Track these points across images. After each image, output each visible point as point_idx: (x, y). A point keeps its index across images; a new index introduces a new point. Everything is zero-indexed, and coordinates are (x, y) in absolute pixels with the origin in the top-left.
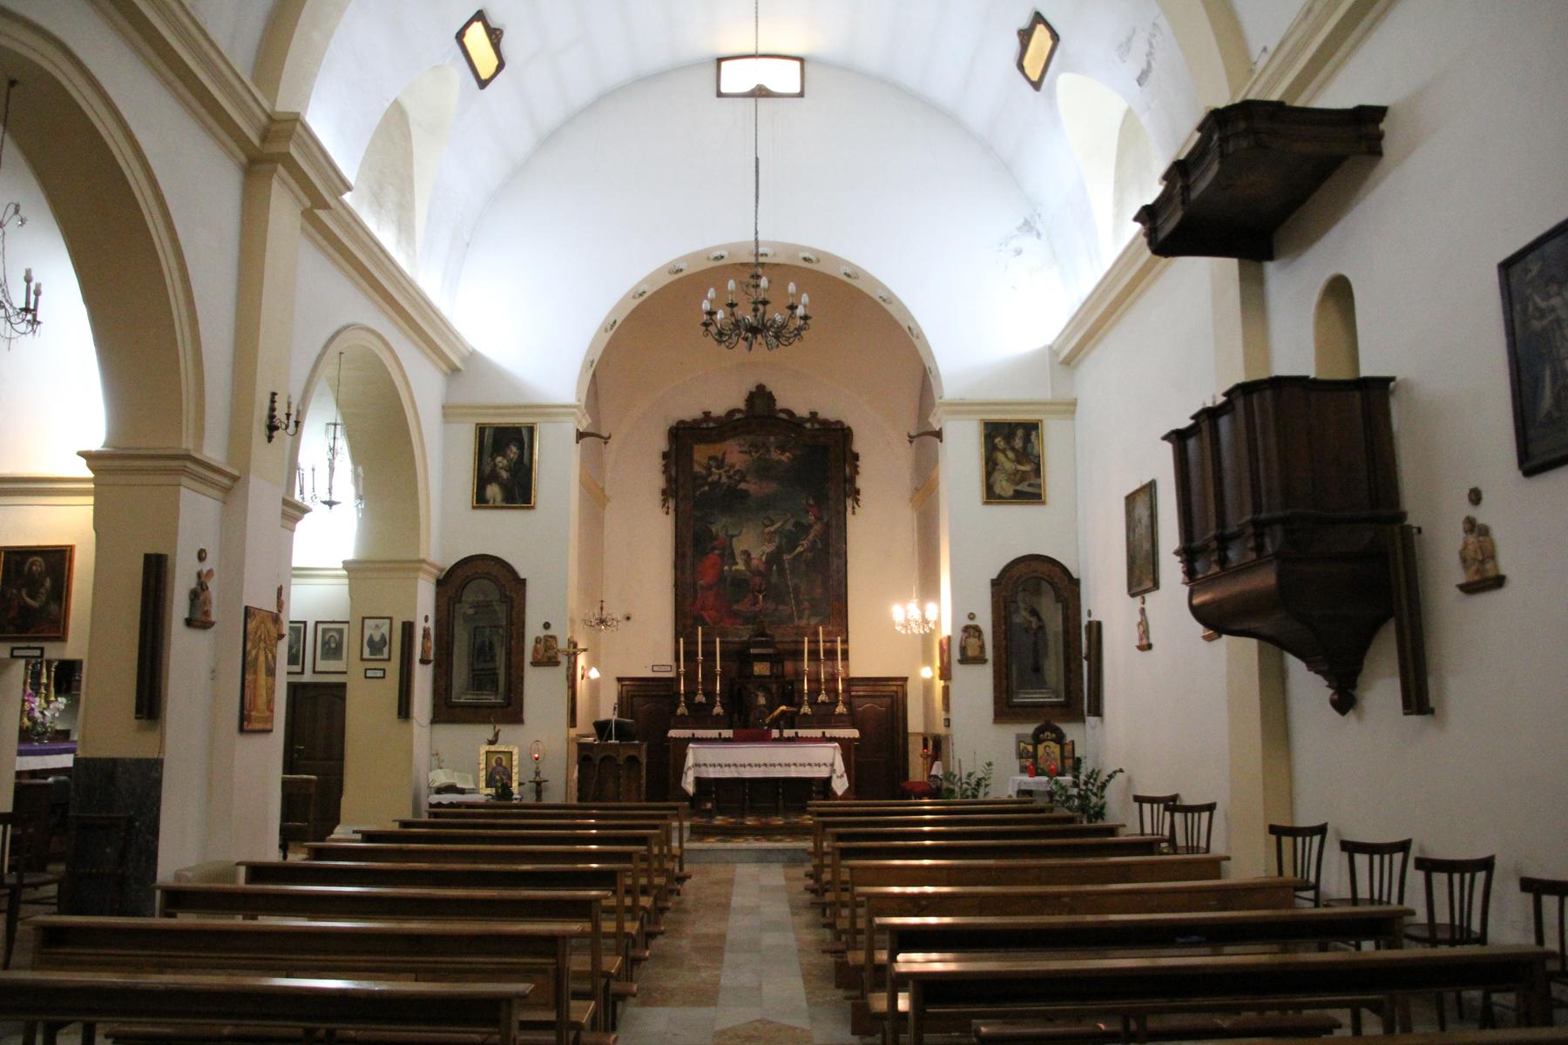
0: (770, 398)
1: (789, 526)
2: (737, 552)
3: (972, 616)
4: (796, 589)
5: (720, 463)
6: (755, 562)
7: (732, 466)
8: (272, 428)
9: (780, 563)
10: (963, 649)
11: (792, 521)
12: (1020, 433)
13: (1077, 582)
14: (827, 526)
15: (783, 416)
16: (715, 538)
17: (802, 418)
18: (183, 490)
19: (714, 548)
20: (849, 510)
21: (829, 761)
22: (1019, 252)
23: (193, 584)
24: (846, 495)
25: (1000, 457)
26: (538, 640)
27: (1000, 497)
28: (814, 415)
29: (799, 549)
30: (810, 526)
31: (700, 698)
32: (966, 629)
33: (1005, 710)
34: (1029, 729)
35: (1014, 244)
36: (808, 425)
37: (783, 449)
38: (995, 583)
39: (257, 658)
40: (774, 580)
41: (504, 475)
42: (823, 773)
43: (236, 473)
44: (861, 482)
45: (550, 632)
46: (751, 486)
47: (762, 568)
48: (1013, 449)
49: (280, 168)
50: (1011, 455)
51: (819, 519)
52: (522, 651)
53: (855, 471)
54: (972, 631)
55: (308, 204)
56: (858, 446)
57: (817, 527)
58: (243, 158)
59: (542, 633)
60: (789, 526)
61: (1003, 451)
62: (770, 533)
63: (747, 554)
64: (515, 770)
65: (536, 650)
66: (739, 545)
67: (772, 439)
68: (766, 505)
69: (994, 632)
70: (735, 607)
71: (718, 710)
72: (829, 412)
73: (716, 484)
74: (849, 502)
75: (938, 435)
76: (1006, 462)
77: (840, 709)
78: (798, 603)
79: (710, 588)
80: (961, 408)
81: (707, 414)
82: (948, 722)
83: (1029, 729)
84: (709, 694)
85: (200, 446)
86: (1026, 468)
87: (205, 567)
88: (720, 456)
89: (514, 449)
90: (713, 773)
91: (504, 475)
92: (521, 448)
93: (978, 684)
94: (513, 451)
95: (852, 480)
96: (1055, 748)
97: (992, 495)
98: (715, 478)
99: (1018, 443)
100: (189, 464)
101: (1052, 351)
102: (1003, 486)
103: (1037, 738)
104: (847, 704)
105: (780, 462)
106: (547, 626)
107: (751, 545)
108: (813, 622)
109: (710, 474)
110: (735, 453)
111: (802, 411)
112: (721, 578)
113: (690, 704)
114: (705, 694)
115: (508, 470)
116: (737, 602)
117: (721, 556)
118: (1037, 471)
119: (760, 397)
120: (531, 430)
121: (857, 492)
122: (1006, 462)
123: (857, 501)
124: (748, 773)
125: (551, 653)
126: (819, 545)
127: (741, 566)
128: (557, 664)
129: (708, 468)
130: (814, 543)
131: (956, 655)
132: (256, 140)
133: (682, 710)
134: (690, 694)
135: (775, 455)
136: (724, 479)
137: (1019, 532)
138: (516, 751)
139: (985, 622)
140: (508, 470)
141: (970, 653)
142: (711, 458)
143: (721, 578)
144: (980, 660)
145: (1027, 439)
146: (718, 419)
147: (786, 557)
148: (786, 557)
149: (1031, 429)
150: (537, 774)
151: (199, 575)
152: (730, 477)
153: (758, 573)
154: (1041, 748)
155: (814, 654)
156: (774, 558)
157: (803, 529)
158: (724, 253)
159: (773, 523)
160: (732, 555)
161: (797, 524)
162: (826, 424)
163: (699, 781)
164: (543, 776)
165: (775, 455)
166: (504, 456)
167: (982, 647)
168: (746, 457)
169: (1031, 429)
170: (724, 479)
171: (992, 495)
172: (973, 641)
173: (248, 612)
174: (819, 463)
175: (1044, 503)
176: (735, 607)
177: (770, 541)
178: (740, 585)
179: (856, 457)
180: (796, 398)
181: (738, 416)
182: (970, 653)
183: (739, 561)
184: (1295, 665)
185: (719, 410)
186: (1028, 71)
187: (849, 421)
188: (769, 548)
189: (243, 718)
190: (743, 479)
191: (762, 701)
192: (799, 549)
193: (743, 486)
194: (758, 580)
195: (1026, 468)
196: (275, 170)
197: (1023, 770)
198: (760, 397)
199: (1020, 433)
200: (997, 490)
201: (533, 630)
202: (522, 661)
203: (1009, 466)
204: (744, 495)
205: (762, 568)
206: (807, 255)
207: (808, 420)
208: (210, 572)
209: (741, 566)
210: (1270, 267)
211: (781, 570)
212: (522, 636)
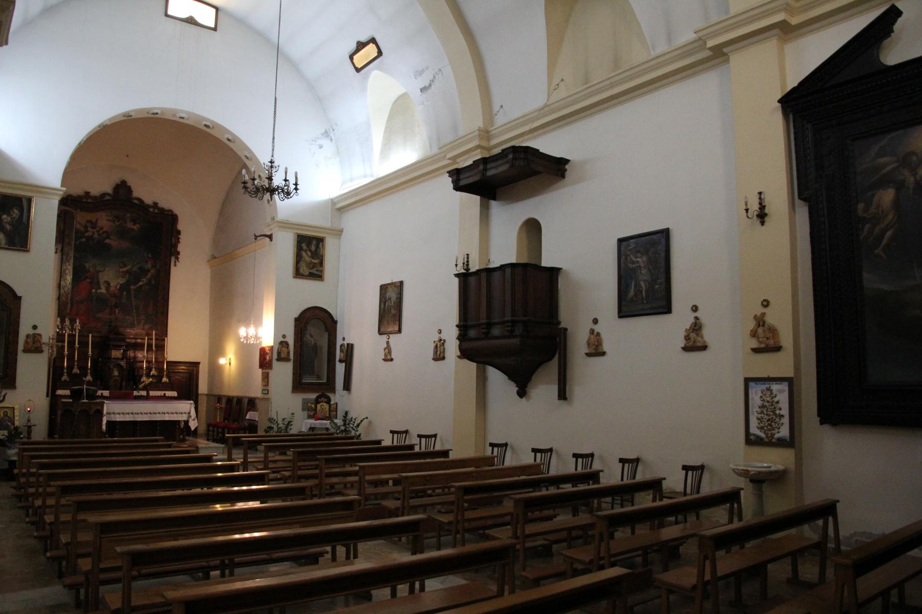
0: (129, 190)
1: (135, 269)
2: (102, 281)
3: (284, 336)
5: (94, 225)
6: (112, 289)
7: (102, 228)
10: (279, 353)
12: (314, 242)
13: (336, 322)
15: (136, 202)
17: (148, 205)
19: (86, 278)
20: (172, 263)
21: (187, 411)
22: (321, 147)
24: (171, 255)
25: (304, 254)
26: (28, 336)
27: (302, 275)
28: (155, 204)
29: (141, 283)
30: (149, 271)
31: (76, 370)
32: (281, 343)
33: (298, 386)
34: (313, 396)
35: (319, 142)
36: (151, 210)
37: (134, 222)
38: (296, 320)
41: (8, 227)
42: (184, 417)
44: (180, 248)
45: (37, 331)
46: (113, 242)
48: (310, 251)
50: (309, 253)
52: (17, 343)
53: (178, 241)
54: (283, 344)
56: (180, 227)
59: (31, 332)
61: (306, 251)
63: (108, 283)
64: (16, 418)
65: (26, 342)
67: (129, 215)
69: (295, 346)
70: (98, 315)
71: (89, 378)
72: (164, 204)
73: (87, 238)
74: (173, 259)
75: (270, 237)
76: (306, 256)
77: (165, 379)
80: (286, 225)
81: (87, 193)
82: (266, 391)
83: (313, 396)
84: (83, 369)
86: (316, 261)
88: (94, 220)
89: (16, 211)
90: (118, 418)
91: (8, 227)
92: (22, 211)
93: (283, 373)
94: (16, 212)
95: (176, 246)
96: (326, 406)
97: (298, 274)
98: (90, 234)
99: (313, 248)
101: (333, 202)
102: (304, 270)
103: (317, 401)
104: (168, 376)
105: (132, 229)
106: (35, 327)
107: (111, 278)
108: (147, 327)
109: (87, 231)
110: (104, 220)
111: (148, 200)
113: (69, 373)
114: (79, 368)
115: (11, 224)
118: (321, 263)
119: (123, 188)
120: (29, 200)
121: (178, 253)
122: (306, 256)
123: (177, 258)
124: (139, 418)
125: (38, 345)
126: (153, 282)
127: (103, 290)
128: (41, 351)
129: (86, 227)
130: (150, 281)
131: (275, 356)
133: (65, 377)
134: (70, 367)
135: (130, 225)
136: (96, 236)
137: (310, 294)
138: (16, 407)
139: (291, 340)
140: (11, 224)
141: (283, 356)
142: (88, 222)
144: (287, 359)
145: (317, 247)
146: (95, 198)
147: (132, 287)
148: (132, 287)
149: (320, 241)
150: (29, 421)
152: (99, 235)
154: (319, 406)
155: (150, 346)
156: (124, 288)
157: (144, 272)
158: (159, 112)
159: (125, 266)
160: (98, 283)
161: (141, 268)
162: (162, 210)
163: (109, 423)
164: (32, 422)
165: (130, 225)
166: (9, 215)
167: (288, 353)
168: (111, 224)
169: (320, 241)
170: (96, 236)
171: (298, 274)
172: (284, 349)
174: (156, 235)
175: (323, 280)
176: (98, 315)
177: (123, 277)
179: (179, 233)
180: (145, 192)
181: (108, 198)
182: (283, 356)
183: (102, 286)
184: (495, 375)
185: (95, 191)
186: (355, 61)
187: (177, 211)
188: (122, 281)
190: (108, 237)
191: (116, 373)
192: (141, 283)
193: (107, 241)
195: (316, 261)
197: (309, 417)
198: (123, 188)
199: (314, 242)
200: (301, 271)
201: (25, 330)
202: (17, 349)
203: (308, 259)
206: (208, 124)
207: (151, 207)
209: (103, 290)
210: (493, 203)
212: (16, 333)
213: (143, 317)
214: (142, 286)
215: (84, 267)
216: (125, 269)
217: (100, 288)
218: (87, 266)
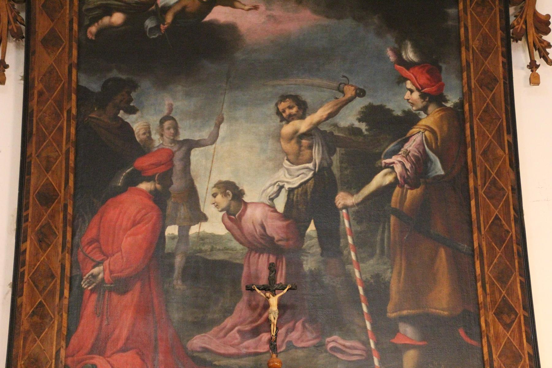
1: (350, 118)
2: (204, 188)
4: (378, 291)
6: (254, 215)
9: (328, 217)
11: (360, 104)
14: (457, 116)
16: (143, 149)
29: (381, 179)
30: (410, 120)
40: (309, 264)
47: (275, 228)
51: (435, 98)
57: (430, 119)
60: (350, 118)
62: (299, 137)
63: (233, 192)
66: (209, 169)
68: (290, 60)
70: (197, 342)
74: (520, 56)
78: (385, 328)
79: (121, 286)
112: (157, 253)
116: (201, 326)
117: (159, 198)
123: (542, 49)
126: (438, 169)
127: (214, 225)
130: (421, 163)
143: (157, 253)
147: (343, 199)
148: (343, 199)
153: (263, 244)
156: (311, 204)
157: (391, 126)
159: (304, 110)
160: (191, 194)
161: (375, 115)
176: (197, 342)
178: (212, 276)
183: (208, 208)
188: (296, 176)
192: (381, 179)
194: (262, 263)
204: (223, 41)
205: (275, 228)
209: (214, 225)
211: (330, 238)
213: (408, 332)
214: (385, 192)
215: (127, 129)
216: (303, 126)
217: (204, 218)
218: (137, 124)
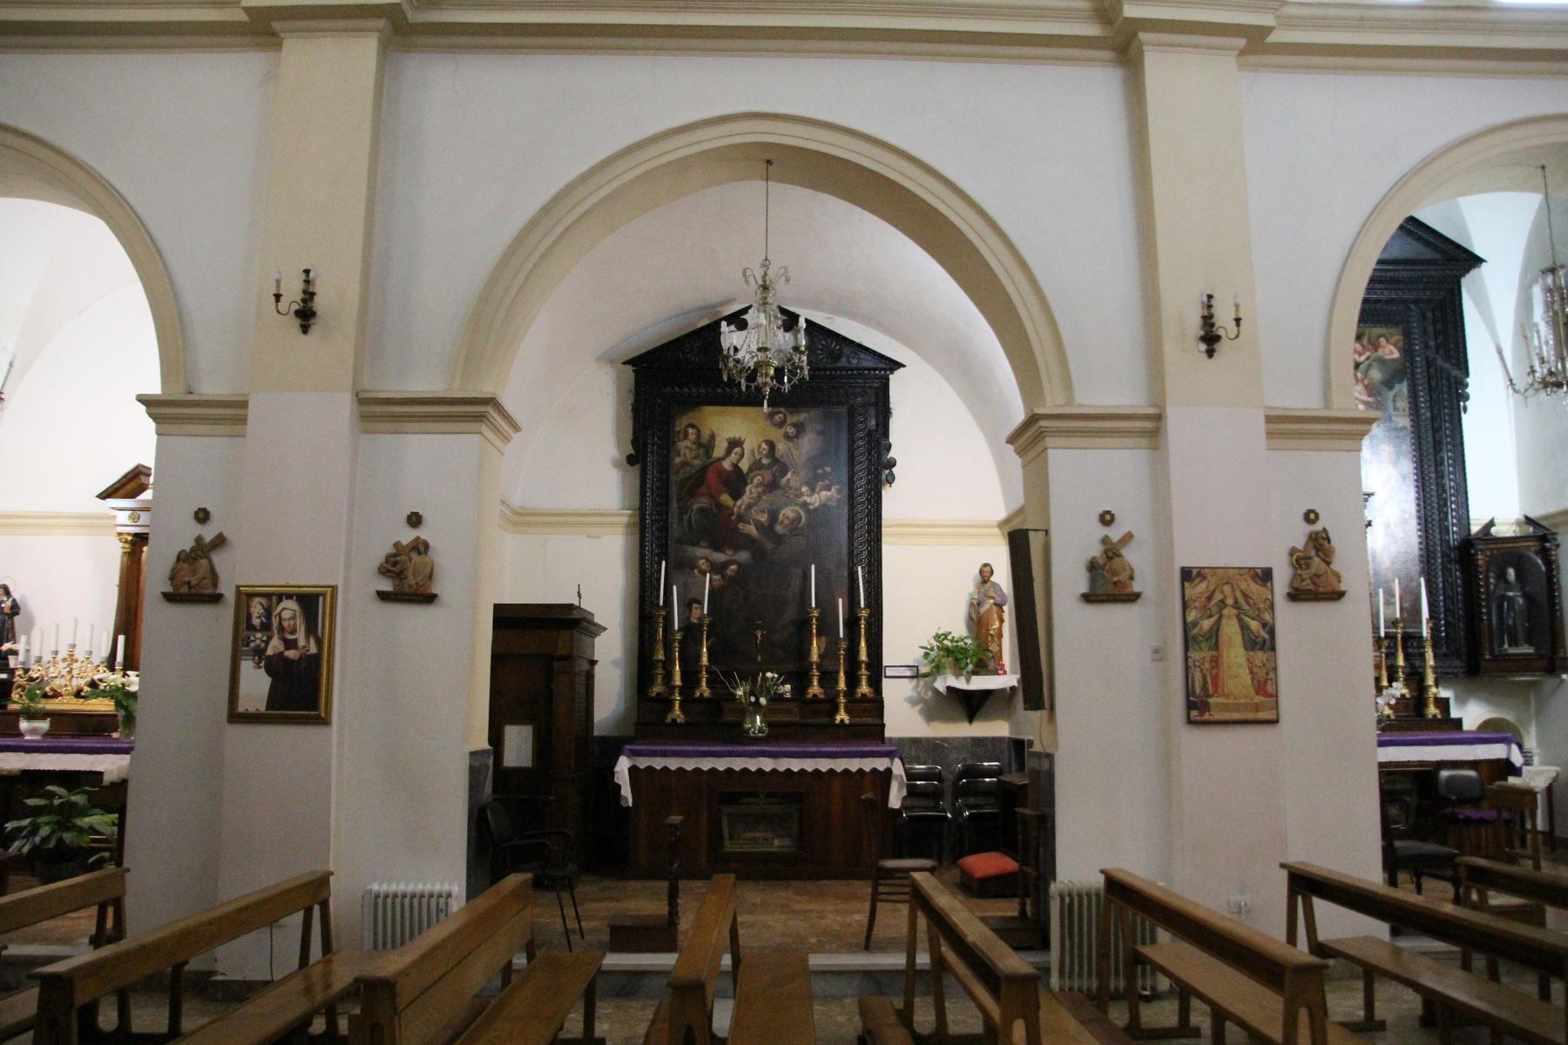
8: (1210, 339)
18: (1051, 453)
23: (1096, 551)
39: (1216, 631)
43: (1151, 411)
49: (1142, 36)
55: (1241, 42)
58: (1107, 55)
85: (1070, 399)
87: (1115, 534)
100: (1043, 423)
132: (1091, 30)
151: (1105, 540)
173: (1187, 575)
189: (1190, 706)
196: (1141, 44)
208: (1129, 537)
